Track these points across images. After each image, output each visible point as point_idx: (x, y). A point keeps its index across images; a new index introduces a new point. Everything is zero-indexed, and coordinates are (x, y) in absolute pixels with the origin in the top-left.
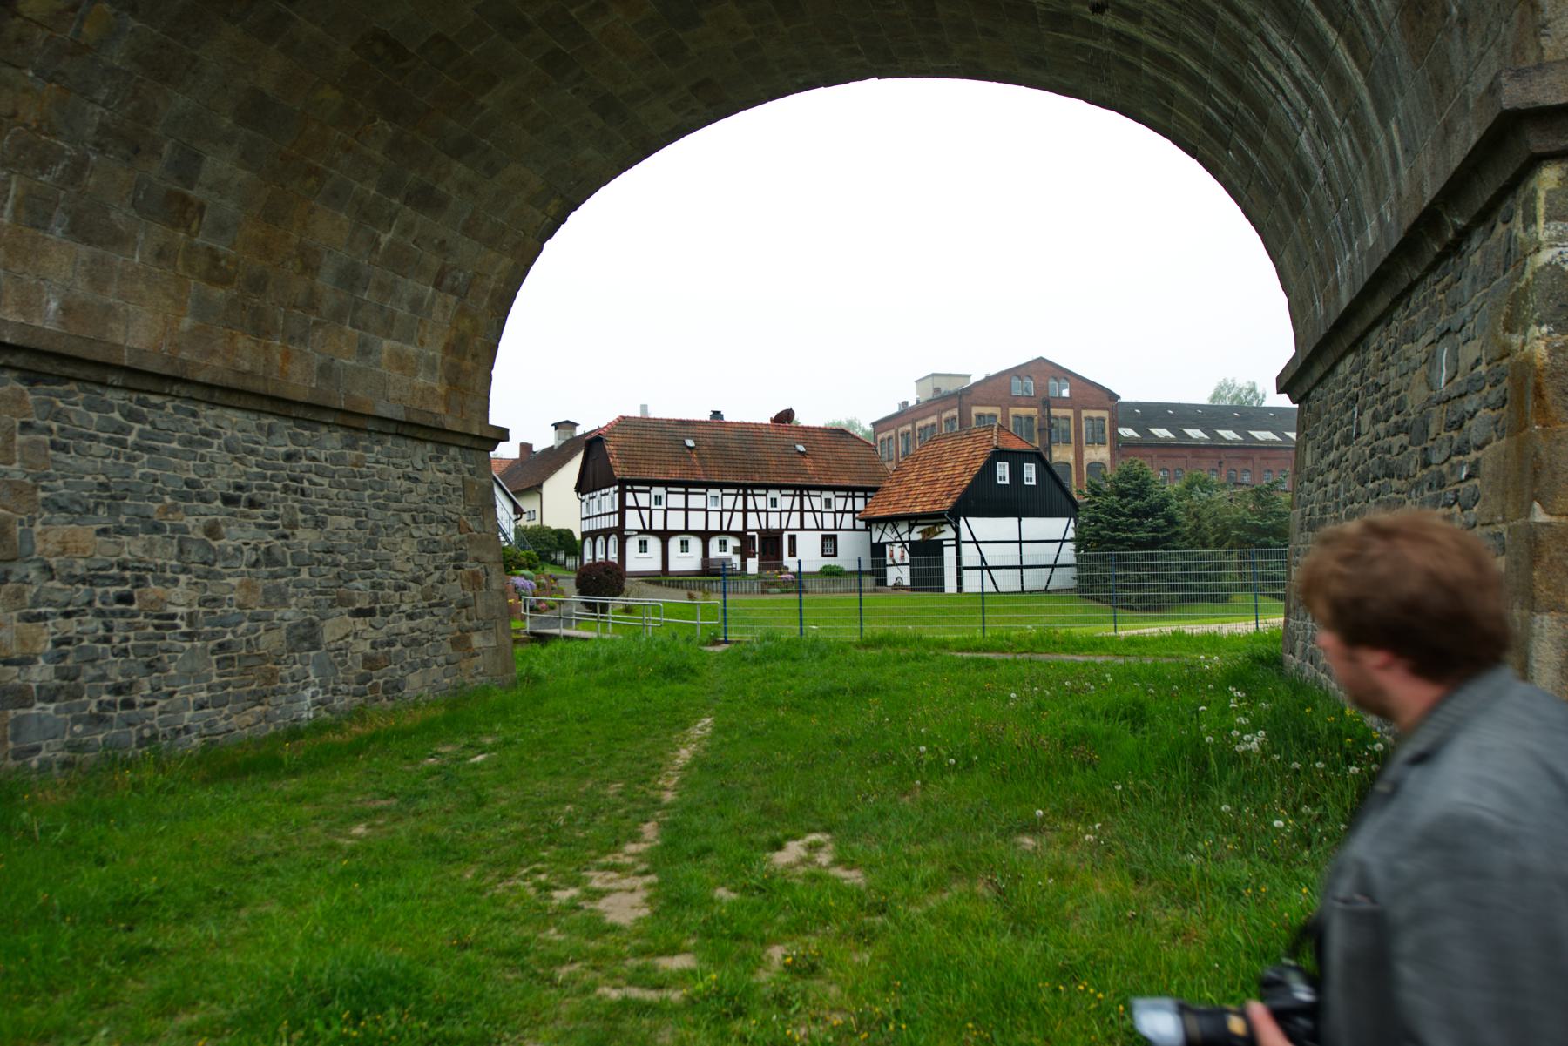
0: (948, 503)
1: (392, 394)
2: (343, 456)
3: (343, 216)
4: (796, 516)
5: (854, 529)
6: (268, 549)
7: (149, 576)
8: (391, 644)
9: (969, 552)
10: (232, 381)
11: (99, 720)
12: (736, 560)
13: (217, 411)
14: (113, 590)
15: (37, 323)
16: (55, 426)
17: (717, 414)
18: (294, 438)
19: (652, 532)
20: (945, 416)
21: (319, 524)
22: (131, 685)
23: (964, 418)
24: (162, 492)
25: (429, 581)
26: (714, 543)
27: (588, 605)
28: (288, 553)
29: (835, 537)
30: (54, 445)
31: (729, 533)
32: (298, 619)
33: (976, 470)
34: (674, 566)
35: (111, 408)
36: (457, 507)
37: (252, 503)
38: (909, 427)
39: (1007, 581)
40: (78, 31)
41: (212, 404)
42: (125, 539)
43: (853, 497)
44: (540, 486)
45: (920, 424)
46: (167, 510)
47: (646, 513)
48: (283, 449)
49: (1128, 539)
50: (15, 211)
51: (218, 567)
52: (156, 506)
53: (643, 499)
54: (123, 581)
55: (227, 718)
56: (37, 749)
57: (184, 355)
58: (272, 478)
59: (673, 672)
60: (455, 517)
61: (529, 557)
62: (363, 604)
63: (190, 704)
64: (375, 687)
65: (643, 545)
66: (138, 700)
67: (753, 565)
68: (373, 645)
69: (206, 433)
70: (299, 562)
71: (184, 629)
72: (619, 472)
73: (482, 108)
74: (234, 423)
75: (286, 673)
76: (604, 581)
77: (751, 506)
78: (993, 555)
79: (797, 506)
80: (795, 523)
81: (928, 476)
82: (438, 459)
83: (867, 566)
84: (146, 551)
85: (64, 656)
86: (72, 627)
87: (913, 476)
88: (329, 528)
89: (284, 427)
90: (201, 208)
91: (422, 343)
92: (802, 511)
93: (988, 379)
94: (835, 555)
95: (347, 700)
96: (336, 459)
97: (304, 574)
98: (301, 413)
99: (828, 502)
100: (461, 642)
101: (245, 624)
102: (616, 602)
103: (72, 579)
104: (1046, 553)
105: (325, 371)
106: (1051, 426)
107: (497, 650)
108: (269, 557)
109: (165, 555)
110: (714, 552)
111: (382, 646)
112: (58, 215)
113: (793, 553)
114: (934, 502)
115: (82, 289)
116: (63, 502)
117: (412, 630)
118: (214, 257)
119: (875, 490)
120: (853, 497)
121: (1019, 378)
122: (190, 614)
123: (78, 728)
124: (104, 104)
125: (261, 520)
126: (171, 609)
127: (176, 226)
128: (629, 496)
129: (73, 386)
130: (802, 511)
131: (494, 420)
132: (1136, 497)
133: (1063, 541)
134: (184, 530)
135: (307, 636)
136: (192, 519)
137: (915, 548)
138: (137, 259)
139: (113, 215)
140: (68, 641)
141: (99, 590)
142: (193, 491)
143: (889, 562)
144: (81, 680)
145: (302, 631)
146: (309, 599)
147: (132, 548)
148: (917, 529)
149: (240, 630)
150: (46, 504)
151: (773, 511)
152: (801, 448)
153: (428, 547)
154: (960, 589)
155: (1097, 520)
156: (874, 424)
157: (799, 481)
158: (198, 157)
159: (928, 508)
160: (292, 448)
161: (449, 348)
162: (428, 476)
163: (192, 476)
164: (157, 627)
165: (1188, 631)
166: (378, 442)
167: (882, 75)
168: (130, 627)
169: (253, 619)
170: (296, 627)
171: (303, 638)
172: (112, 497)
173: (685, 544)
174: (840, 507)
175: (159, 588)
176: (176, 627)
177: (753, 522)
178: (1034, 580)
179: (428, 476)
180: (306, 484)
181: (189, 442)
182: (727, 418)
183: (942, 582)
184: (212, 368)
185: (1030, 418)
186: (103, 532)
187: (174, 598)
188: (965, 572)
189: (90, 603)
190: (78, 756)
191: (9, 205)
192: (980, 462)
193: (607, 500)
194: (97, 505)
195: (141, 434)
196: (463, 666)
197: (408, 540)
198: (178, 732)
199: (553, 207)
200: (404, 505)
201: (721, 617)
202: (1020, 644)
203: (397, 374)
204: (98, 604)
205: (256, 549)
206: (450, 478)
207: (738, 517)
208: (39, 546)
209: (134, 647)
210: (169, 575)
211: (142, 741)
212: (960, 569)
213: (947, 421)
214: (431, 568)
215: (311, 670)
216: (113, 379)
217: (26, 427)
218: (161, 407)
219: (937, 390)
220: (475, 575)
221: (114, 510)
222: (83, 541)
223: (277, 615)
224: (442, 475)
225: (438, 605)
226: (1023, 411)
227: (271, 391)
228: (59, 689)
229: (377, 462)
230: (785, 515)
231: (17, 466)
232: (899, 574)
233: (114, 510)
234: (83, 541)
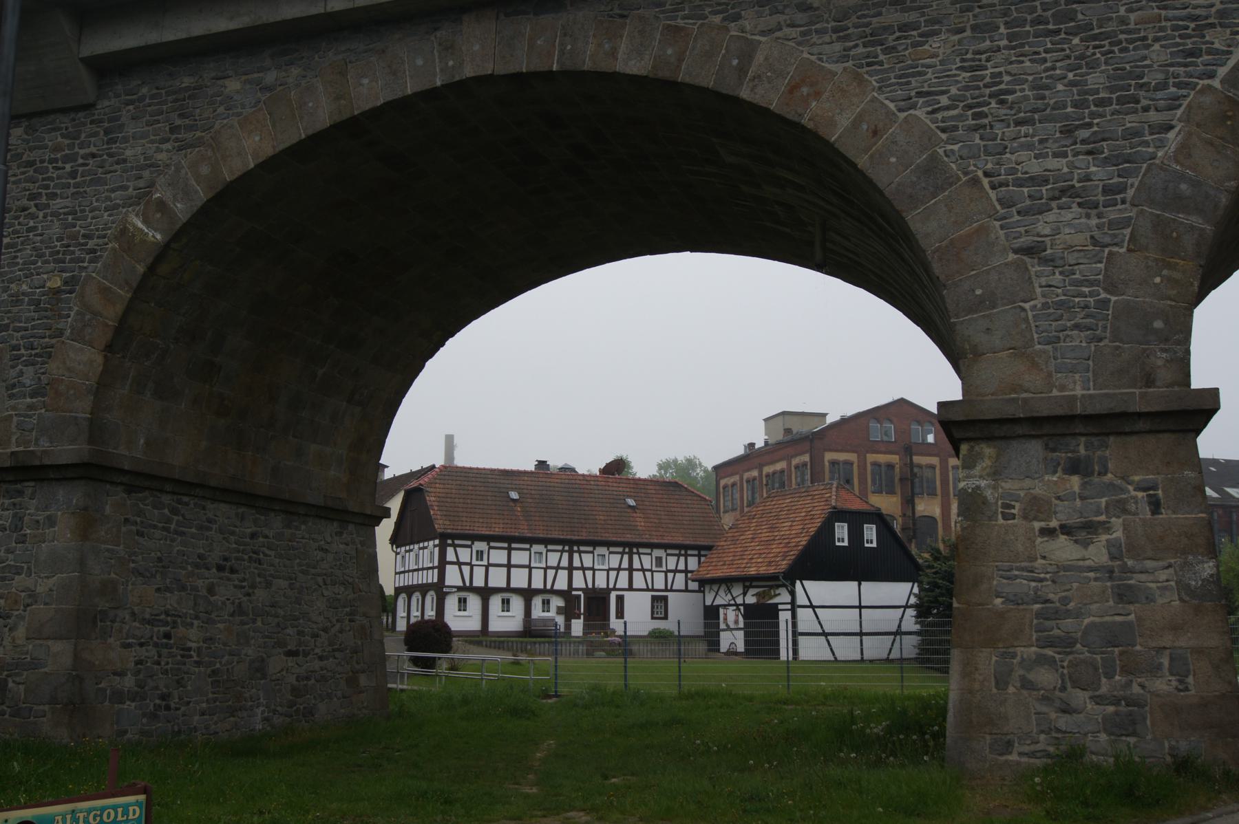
0: (784, 565)
4: (624, 575)
5: (686, 590)
8: (308, 678)
9: (805, 615)
11: (154, 716)
12: (560, 620)
16: (138, 520)
17: (542, 464)
20: (795, 461)
23: (816, 461)
25: (333, 630)
26: (537, 602)
27: (415, 661)
29: (665, 599)
33: (813, 530)
34: (496, 625)
37: (233, 571)
38: (755, 473)
39: (847, 649)
41: (214, 500)
42: (168, 595)
43: (686, 556)
45: (768, 469)
47: (466, 569)
48: (249, 531)
51: (213, 616)
53: (464, 555)
54: (167, 624)
55: (216, 723)
60: (351, 580)
65: (463, 603)
66: (173, 706)
67: (577, 627)
69: (210, 521)
71: (195, 658)
74: (223, 512)
75: (247, 695)
76: (431, 637)
77: (577, 563)
79: (625, 564)
80: (623, 582)
82: (341, 534)
83: (700, 631)
85: (139, 671)
87: (749, 535)
92: (631, 570)
93: (844, 421)
94: (666, 618)
97: (259, 623)
99: (659, 560)
100: (352, 681)
101: (226, 658)
104: (889, 620)
106: (914, 475)
108: (240, 610)
110: (537, 612)
113: (620, 614)
119: (709, 548)
120: (686, 556)
122: (199, 648)
123: (144, 720)
125: (236, 582)
126: (190, 644)
128: (450, 550)
129: (147, 493)
130: (631, 570)
133: (906, 607)
135: (259, 669)
137: (750, 612)
141: (156, 629)
143: (722, 626)
148: (752, 591)
151: (600, 569)
152: (631, 502)
154: (795, 652)
156: (716, 468)
157: (629, 538)
159: (763, 570)
160: (255, 529)
163: (202, 551)
167: (693, 249)
173: (506, 604)
174: (672, 566)
176: (191, 657)
177: (578, 582)
178: (875, 648)
180: (261, 556)
185: (890, 466)
186: (158, 590)
192: (818, 523)
193: (427, 553)
205: (233, 603)
207: (563, 575)
210: (189, 620)
212: (796, 634)
213: (797, 467)
214: (334, 621)
218: (187, 504)
219: (788, 431)
224: (342, 546)
225: (338, 650)
226: (882, 458)
232: (733, 638)
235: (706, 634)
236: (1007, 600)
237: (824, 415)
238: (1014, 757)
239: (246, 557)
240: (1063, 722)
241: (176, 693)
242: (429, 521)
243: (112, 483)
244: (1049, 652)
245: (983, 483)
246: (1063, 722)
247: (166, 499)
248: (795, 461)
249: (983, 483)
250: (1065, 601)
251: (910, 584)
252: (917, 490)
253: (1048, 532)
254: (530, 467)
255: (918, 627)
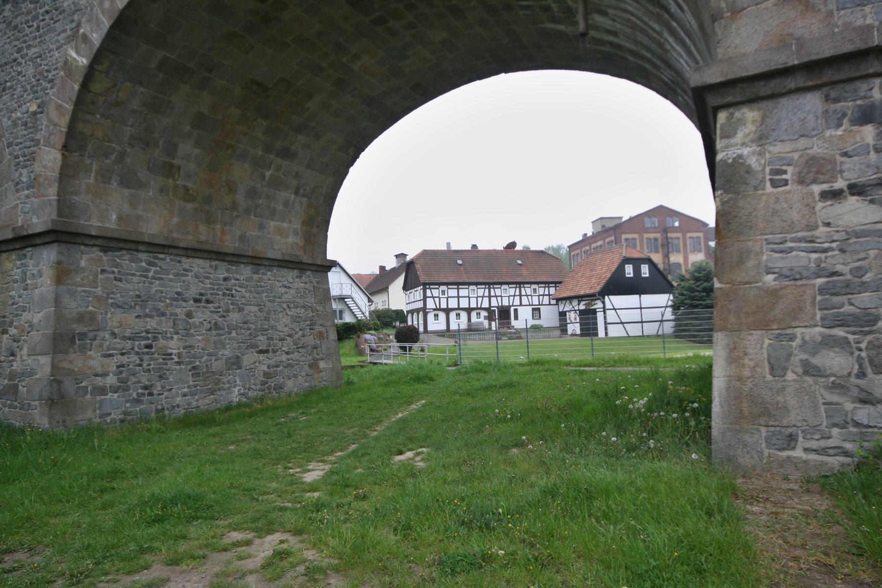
0: (598, 288)
1: (276, 247)
2: (252, 278)
3: (247, 165)
4: (517, 299)
5: (550, 304)
6: (216, 323)
7: (160, 336)
8: (277, 366)
10: (196, 246)
11: (137, 401)
13: (190, 260)
14: (143, 343)
15: (107, 225)
16: (116, 270)
17: (474, 246)
18: (228, 270)
19: (441, 310)
20: (607, 240)
21: (241, 310)
22: (151, 386)
24: (165, 298)
25: (297, 336)
26: (474, 314)
27: (401, 348)
28: (226, 324)
29: (539, 309)
30: (116, 279)
31: (481, 309)
32: (230, 355)
33: (613, 270)
34: (453, 327)
35: (141, 261)
36: (311, 300)
37: (208, 302)
38: (588, 248)
39: (634, 330)
40: (117, 96)
41: (188, 257)
44: (387, 288)
45: (593, 245)
46: (167, 306)
47: (437, 300)
48: (222, 276)
49: (701, 305)
50: (95, 177)
51: (192, 331)
52: (162, 304)
53: (436, 293)
54: (148, 338)
55: (197, 400)
56: (110, 414)
57: (175, 235)
58: (217, 289)
59: (418, 379)
61: (375, 324)
62: (263, 347)
63: (179, 394)
64: (269, 388)
66: (155, 392)
68: (268, 367)
69: (185, 270)
70: (231, 328)
71: (176, 360)
72: (422, 280)
73: (308, 108)
74: (198, 265)
75: (225, 380)
78: (625, 316)
79: (517, 293)
80: (517, 302)
81: (588, 274)
82: (300, 277)
83: (557, 324)
84: (158, 325)
85: (121, 372)
86: (124, 359)
87: (580, 274)
88: (246, 312)
89: (223, 266)
90: (179, 168)
91: (290, 222)
93: (631, 219)
95: (256, 393)
96: (249, 279)
97: (234, 334)
98: (230, 258)
99: (535, 290)
100: (314, 365)
101: (205, 358)
102: (416, 346)
103: (124, 338)
104: (656, 314)
105: (242, 238)
106: (668, 243)
107: (333, 369)
108: (216, 326)
109: (166, 326)
110: (474, 318)
111: (273, 367)
112: (114, 177)
113: (516, 318)
114: (591, 288)
115: (127, 209)
116: (120, 304)
117: (288, 360)
118: (187, 189)
119: (560, 283)
121: (649, 217)
123: (128, 405)
124: (132, 126)
125: (212, 309)
126: (170, 351)
127: (167, 177)
128: (428, 291)
129: (124, 252)
130: (520, 295)
131: (330, 257)
132: (705, 281)
133: (666, 307)
134: (176, 315)
135: (235, 363)
136: (179, 310)
138: (151, 193)
139: (139, 175)
140: (123, 366)
141: (137, 343)
142: (180, 297)
143: (568, 321)
144: (129, 383)
145: (233, 360)
146: (236, 345)
147: (152, 323)
149: (203, 360)
150: (112, 305)
151: (505, 296)
152: (519, 262)
153: (296, 319)
154: (606, 334)
155: (682, 294)
156: (569, 247)
157: (519, 280)
158: (176, 146)
159: (588, 292)
160: (227, 275)
161: (304, 223)
162: (296, 285)
163: (179, 290)
164: (164, 359)
165: (702, 354)
166: (269, 270)
167: (506, 72)
168: (151, 359)
169: (208, 355)
170: (230, 358)
171: (234, 364)
172: (142, 301)
173: (458, 315)
175: (164, 342)
176: (172, 359)
178: (650, 329)
179: (296, 285)
180: (234, 292)
181: (177, 275)
182: (480, 248)
183: (596, 329)
184: (188, 240)
185: (656, 239)
186: (138, 317)
187: (171, 346)
188: (609, 326)
189: (133, 349)
190: (129, 418)
191: (93, 175)
192: (616, 265)
193: (418, 293)
194: (135, 305)
195: (155, 272)
196: (315, 377)
197: (286, 317)
198: (174, 407)
199: (351, 151)
200: (284, 300)
201: (458, 351)
202: (608, 362)
203: (278, 238)
204: (136, 349)
205: (210, 322)
206: (307, 286)
207: (486, 300)
208: (110, 324)
209: (153, 369)
210: (169, 335)
211: (158, 411)
214: (298, 330)
215: (237, 379)
216: (142, 248)
217: (103, 271)
218: (164, 259)
220: (320, 333)
221: (143, 307)
222: (131, 321)
223: (221, 353)
224: (302, 285)
225: (301, 347)
226: (651, 236)
227: (215, 249)
228: (119, 387)
229: (269, 280)
230: (511, 298)
231: (99, 289)
232: (574, 327)
233: (143, 307)
234: (131, 321)
235: (561, 325)
236: (781, 276)
237: (621, 218)
238: (798, 453)
239: (220, 293)
240: (863, 414)
241: (159, 385)
242: (417, 277)
243: (86, 245)
244: (839, 332)
245: (746, 151)
246: (863, 414)
247: (143, 256)
248: (607, 240)
249: (746, 151)
250: (858, 272)
251: (667, 295)
252: (670, 250)
253: (835, 195)
254: (468, 247)
255: (673, 317)
